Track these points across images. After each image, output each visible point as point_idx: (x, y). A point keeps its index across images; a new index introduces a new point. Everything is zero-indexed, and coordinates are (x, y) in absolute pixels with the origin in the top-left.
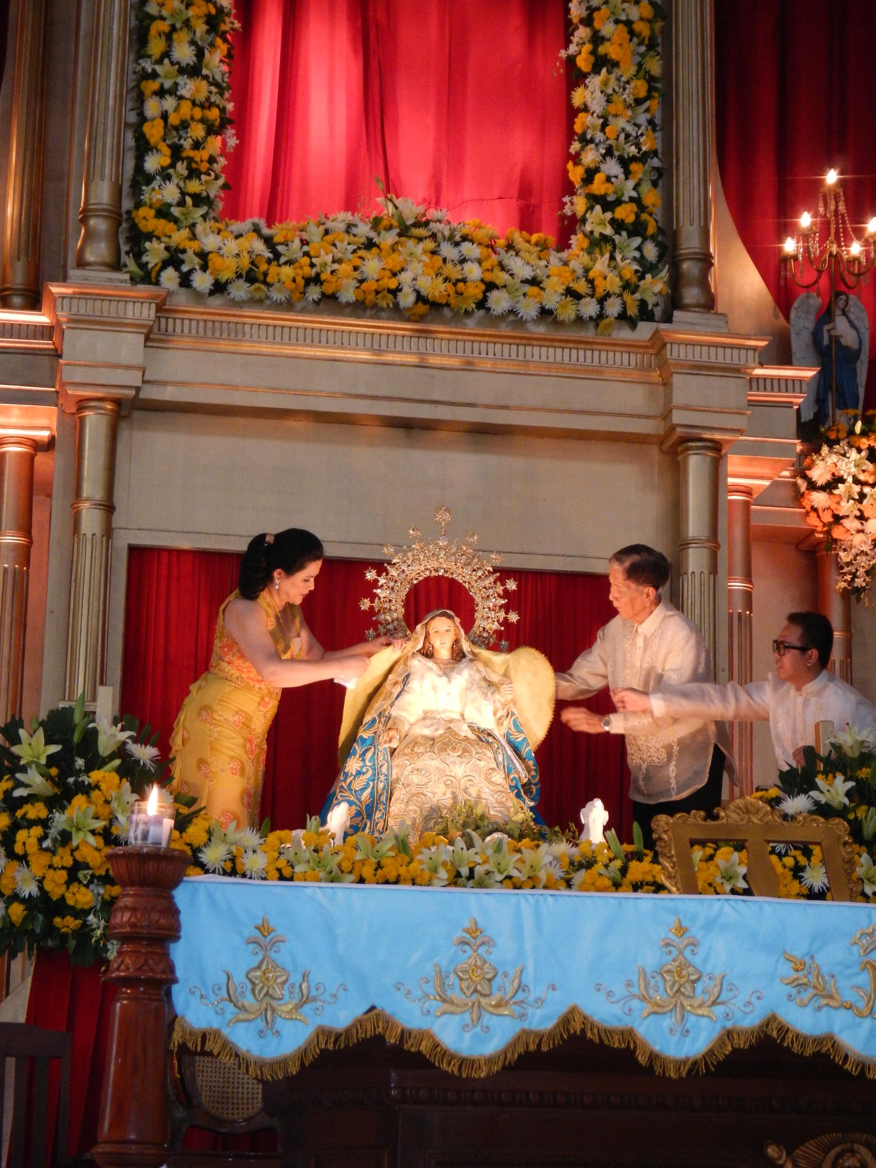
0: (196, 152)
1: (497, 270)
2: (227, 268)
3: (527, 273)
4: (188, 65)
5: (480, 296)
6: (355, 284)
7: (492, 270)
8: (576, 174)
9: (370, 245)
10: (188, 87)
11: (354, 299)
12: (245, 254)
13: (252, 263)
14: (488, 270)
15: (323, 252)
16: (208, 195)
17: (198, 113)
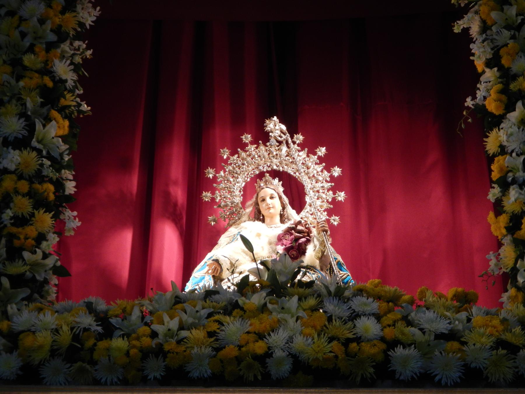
0: (20, 230)
1: (400, 325)
2: (41, 347)
3: (442, 326)
4: (16, 138)
5: (380, 357)
6: (208, 351)
7: (394, 325)
8: (498, 225)
9: (232, 307)
10: (10, 156)
11: (209, 371)
12: (65, 328)
13: (76, 338)
14: (389, 326)
15: (166, 318)
16: (34, 276)
17: (24, 186)
